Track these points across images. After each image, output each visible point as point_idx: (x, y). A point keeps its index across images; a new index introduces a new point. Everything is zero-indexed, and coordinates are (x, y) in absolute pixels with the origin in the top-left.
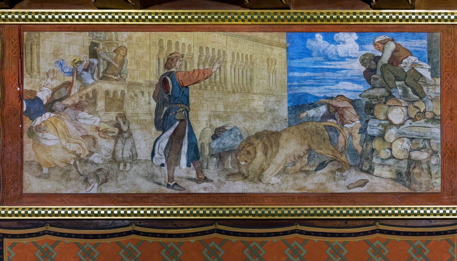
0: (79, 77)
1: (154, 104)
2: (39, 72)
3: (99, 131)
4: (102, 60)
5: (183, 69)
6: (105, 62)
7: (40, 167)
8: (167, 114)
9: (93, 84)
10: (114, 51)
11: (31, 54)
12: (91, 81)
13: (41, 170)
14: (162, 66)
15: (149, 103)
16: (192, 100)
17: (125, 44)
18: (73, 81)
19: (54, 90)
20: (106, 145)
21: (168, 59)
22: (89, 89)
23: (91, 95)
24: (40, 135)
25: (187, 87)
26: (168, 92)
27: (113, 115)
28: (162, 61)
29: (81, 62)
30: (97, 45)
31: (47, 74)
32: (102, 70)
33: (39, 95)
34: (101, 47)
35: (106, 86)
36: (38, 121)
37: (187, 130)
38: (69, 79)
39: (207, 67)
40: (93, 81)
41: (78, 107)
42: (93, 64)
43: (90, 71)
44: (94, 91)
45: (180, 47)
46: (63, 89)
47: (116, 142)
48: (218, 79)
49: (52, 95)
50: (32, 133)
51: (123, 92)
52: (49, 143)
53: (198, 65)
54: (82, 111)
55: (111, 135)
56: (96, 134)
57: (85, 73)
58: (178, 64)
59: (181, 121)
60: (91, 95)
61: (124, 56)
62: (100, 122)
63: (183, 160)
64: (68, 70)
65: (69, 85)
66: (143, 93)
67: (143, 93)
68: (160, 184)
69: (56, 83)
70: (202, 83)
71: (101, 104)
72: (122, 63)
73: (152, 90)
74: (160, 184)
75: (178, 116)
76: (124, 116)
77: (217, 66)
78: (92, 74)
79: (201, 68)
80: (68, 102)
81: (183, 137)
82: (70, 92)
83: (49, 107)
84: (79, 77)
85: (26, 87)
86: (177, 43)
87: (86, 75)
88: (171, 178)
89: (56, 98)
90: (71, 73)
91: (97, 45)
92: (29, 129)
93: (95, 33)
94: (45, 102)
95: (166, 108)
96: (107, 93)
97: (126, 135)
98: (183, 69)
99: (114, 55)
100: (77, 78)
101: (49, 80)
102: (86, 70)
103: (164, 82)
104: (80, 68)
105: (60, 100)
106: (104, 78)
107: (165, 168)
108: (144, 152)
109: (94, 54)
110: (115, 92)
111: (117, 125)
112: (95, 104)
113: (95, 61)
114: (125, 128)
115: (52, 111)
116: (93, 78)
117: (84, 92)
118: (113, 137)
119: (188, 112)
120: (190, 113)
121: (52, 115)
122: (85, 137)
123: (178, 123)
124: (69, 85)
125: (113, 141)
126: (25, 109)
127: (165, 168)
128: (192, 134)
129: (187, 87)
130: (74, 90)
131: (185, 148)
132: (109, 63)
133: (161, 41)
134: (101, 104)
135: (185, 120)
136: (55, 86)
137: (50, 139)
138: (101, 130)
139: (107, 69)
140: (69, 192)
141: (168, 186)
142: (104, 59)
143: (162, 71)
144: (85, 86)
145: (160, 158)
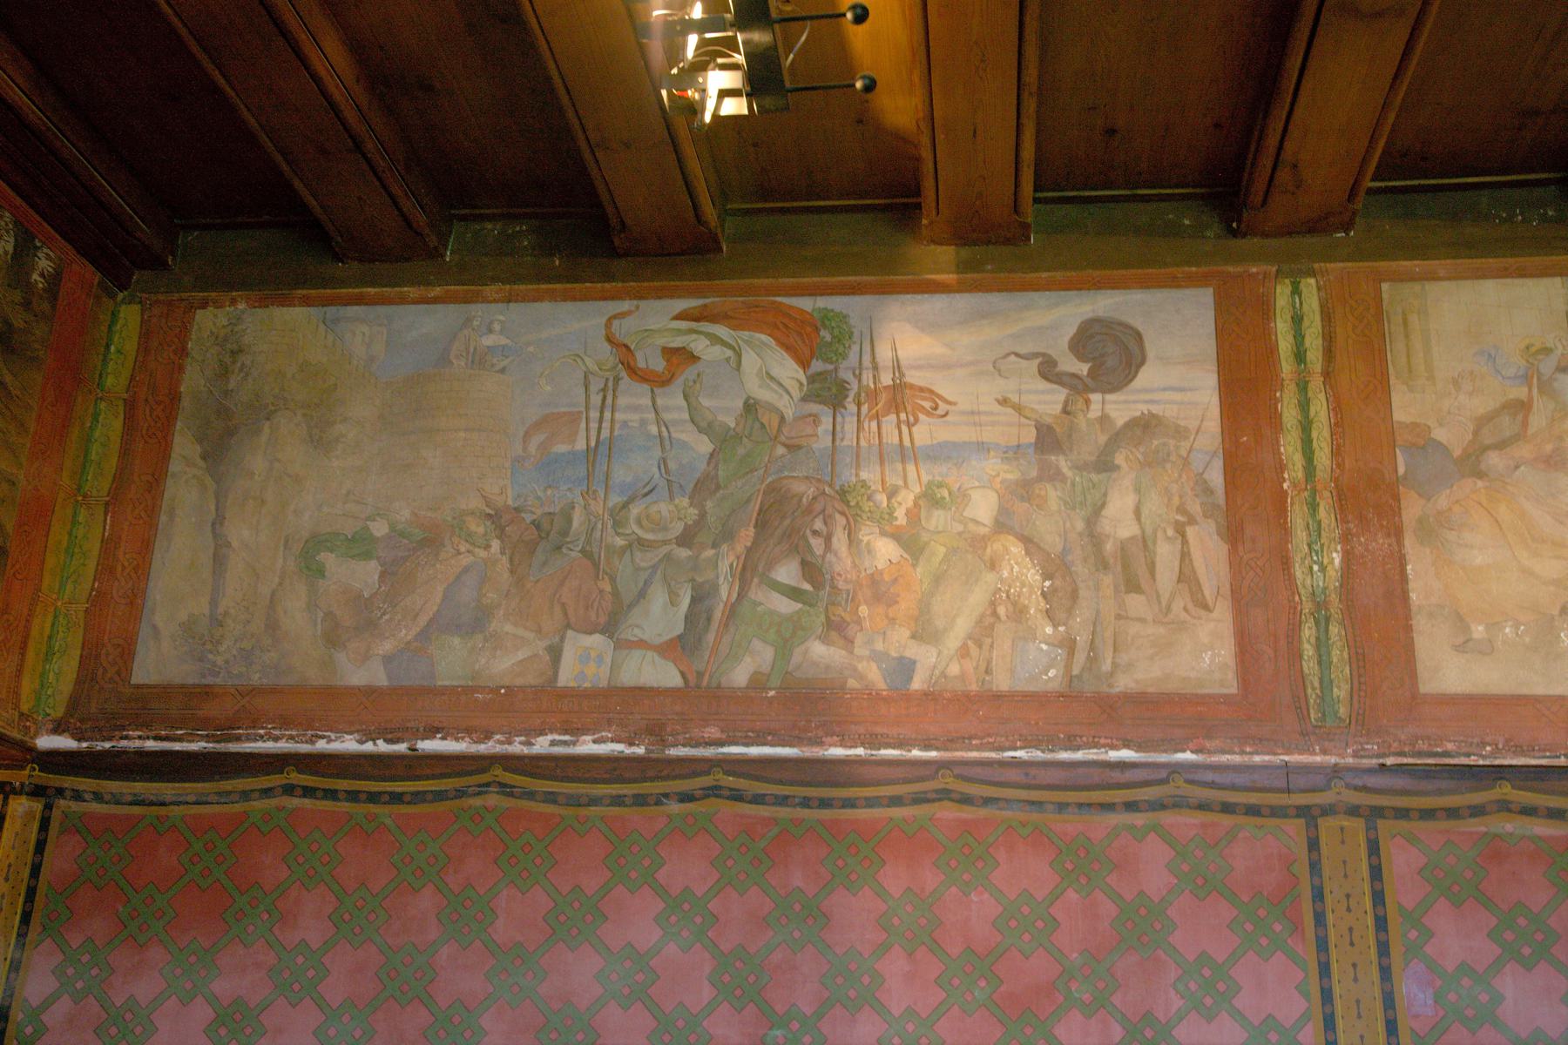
0: (1546, 388)
2: (1431, 378)
7: (1461, 622)
11: (1407, 336)
13: (1466, 629)
18: (1531, 399)
19: (1482, 422)
24: (1452, 536)
29: (1547, 351)
33: (1440, 434)
36: (1442, 501)
38: (1521, 392)
46: (1506, 420)
49: (1476, 433)
50: (1429, 531)
52: (1479, 559)
64: (1511, 372)
65: (1522, 408)
69: (1481, 405)
80: (1524, 451)
82: (1525, 424)
83: (1471, 464)
84: (1546, 388)
85: (1399, 415)
89: (1487, 442)
90: (1526, 379)
92: (1420, 521)
94: (1457, 453)
100: (1541, 391)
104: (1547, 366)
105: (1501, 445)
115: (1481, 475)
121: (1480, 484)
126: (1401, 470)
130: (1537, 421)
136: (1481, 411)
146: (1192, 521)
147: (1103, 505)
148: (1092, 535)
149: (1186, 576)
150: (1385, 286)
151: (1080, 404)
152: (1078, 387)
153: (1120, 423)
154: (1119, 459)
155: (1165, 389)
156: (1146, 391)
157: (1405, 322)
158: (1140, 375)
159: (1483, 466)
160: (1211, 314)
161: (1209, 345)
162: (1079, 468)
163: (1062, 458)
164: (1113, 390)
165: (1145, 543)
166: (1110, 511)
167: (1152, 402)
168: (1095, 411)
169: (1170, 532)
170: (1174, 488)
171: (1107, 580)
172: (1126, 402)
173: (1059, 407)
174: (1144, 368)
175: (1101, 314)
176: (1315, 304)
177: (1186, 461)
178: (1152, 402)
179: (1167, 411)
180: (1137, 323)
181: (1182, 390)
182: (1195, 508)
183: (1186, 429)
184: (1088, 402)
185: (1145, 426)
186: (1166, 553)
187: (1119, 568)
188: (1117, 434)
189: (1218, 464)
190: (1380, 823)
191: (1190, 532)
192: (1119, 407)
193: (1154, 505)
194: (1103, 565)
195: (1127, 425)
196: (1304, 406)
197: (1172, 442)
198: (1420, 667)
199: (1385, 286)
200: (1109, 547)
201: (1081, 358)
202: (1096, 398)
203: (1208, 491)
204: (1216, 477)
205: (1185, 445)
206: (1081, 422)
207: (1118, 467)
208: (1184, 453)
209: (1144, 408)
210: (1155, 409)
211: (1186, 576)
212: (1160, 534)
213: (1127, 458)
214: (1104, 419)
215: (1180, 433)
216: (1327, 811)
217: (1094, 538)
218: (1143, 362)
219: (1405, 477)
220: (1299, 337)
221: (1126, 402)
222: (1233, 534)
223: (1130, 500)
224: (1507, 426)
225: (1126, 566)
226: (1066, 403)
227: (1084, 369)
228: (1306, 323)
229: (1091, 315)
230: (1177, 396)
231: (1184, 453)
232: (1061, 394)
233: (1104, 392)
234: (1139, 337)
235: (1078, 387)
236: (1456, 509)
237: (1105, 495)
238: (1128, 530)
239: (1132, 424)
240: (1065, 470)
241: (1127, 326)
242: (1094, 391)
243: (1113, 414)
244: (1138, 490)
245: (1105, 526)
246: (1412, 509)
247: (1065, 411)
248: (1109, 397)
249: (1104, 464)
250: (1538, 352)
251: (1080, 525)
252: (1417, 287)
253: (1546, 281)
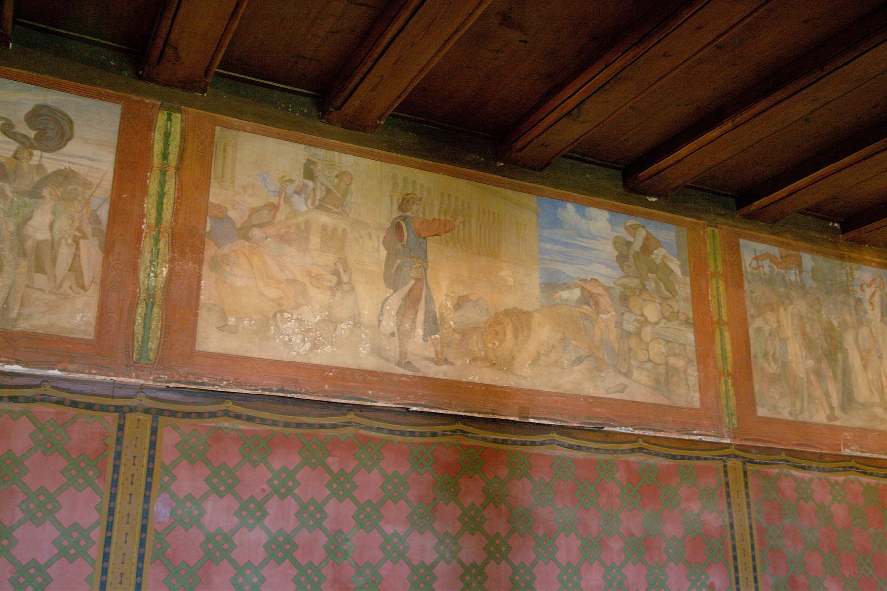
1: (384, 253)
3: (310, 276)
4: (319, 184)
5: (421, 216)
6: (324, 188)
7: (223, 315)
8: (399, 268)
9: (306, 212)
10: (336, 176)
11: (224, 158)
12: (303, 208)
13: (226, 319)
14: (395, 207)
15: (378, 251)
16: (431, 256)
17: (351, 171)
18: (279, 204)
19: (255, 211)
20: (319, 296)
21: (403, 199)
22: (301, 219)
23: (302, 227)
24: (227, 268)
25: (424, 238)
26: (401, 241)
27: (330, 258)
28: (395, 200)
29: (291, 181)
30: (314, 163)
31: (245, 188)
32: (319, 197)
33: (231, 214)
34: (320, 167)
35: (324, 218)
36: (226, 250)
37: (424, 294)
38: (275, 200)
39: (449, 218)
40: (306, 209)
41: (284, 239)
42: (308, 187)
43: (303, 195)
44: (307, 222)
45: (418, 187)
47: (333, 295)
48: (461, 236)
49: (250, 217)
50: (217, 264)
51: (344, 230)
52: (239, 283)
53: (439, 213)
54: (290, 246)
55: (325, 283)
56: (306, 280)
57: (296, 196)
58: (415, 207)
59: (418, 280)
60: (302, 227)
61: (348, 185)
62: (313, 264)
63: (420, 332)
65: (274, 208)
66: (370, 237)
67: (370, 237)
68: (388, 360)
70: (443, 236)
71: (315, 240)
72: (345, 194)
73: (383, 235)
74: (388, 360)
75: (414, 274)
76: (345, 263)
77: (460, 219)
78: (306, 200)
79: (442, 218)
80: (271, 230)
81: (418, 301)
82: (274, 217)
83: (244, 232)
84: (288, 200)
85: (212, 199)
86: (414, 183)
87: (298, 200)
88: (403, 354)
89: (255, 222)
90: (279, 193)
91: (314, 163)
92: (213, 258)
93: (313, 149)
94: (238, 225)
95: (398, 261)
96: (324, 227)
97: (346, 287)
98: (421, 216)
99: (336, 181)
100: (285, 201)
101: (246, 196)
102: (298, 192)
103: (397, 227)
104: (290, 189)
105: (261, 225)
106: (321, 207)
107: (396, 339)
108: (368, 311)
109: (309, 173)
110: (335, 229)
111: (336, 273)
112: (307, 239)
113: (311, 184)
114: (345, 278)
115: (248, 239)
116: (307, 205)
117: (294, 221)
118: (330, 288)
119: (425, 270)
120: (428, 272)
121: (247, 244)
122: (293, 281)
123: (413, 282)
124: (274, 208)
125: (329, 293)
126: (208, 229)
127: (396, 339)
128: (429, 300)
129: (424, 238)
130: (281, 216)
131: (421, 316)
132: (328, 190)
133: (395, 176)
134: (315, 240)
135: (421, 280)
136: (254, 206)
137: (240, 277)
138: (313, 275)
139: (325, 197)
140: (264, 356)
141: (399, 364)
142: (322, 184)
143: (396, 214)
144: (295, 213)
145: (389, 324)
146: (84, 237)
147: (30, 218)
148: (18, 234)
149: (75, 268)
150: (218, 128)
151: (26, 154)
152: (26, 144)
153: (50, 171)
154: (46, 192)
155: (82, 157)
156: (69, 155)
157: (225, 151)
158: (68, 145)
159: (250, 235)
160: (118, 120)
161: (114, 138)
162: (17, 192)
163: (7, 185)
164: (47, 151)
165: (53, 245)
166: (34, 222)
167: (73, 163)
168: (35, 161)
169: (70, 241)
170: (77, 216)
171: (24, 263)
172: (56, 159)
173: (12, 153)
174: (70, 142)
175: (49, 103)
176: (179, 129)
177: (88, 202)
178: (73, 163)
179: (81, 170)
180: (71, 114)
181: (92, 160)
182: (88, 230)
183: (91, 183)
184: (31, 154)
185: (66, 176)
186: (65, 253)
187: (33, 257)
188: (47, 178)
189: (107, 207)
190: (161, 418)
191: (82, 243)
192: (52, 162)
193: (63, 223)
194: (24, 254)
195: (54, 173)
196: (162, 184)
197: (80, 189)
198: (198, 336)
199: (218, 128)
200: (29, 243)
201: (32, 127)
202: (37, 153)
203: (97, 221)
204: (104, 214)
205: (89, 192)
206: (25, 166)
207: (44, 197)
208: (87, 197)
209: (67, 166)
210: (74, 167)
211: (75, 268)
212: (63, 241)
213: (50, 193)
214: (40, 167)
215: (87, 184)
216: (132, 410)
217: (20, 236)
218: (71, 138)
219: (210, 233)
220: (166, 145)
221: (56, 159)
222: (108, 248)
223: (48, 218)
224: (266, 215)
225: (38, 257)
226: (16, 152)
227: (32, 134)
228: (171, 138)
229: (42, 103)
230: (89, 163)
231: (87, 197)
232: (13, 146)
233: (43, 150)
234: (71, 122)
235: (26, 144)
236: (233, 254)
237: (32, 212)
238: (43, 235)
239: (58, 173)
240: (8, 192)
241: (61, 113)
242: (35, 148)
243: (47, 165)
244: (54, 213)
245: (29, 230)
246: (210, 250)
247: (15, 157)
248: (45, 154)
249: (35, 193)
250: (286, 181)
251: (12, 228)
252: (234, 132)
253: (297, 145)
